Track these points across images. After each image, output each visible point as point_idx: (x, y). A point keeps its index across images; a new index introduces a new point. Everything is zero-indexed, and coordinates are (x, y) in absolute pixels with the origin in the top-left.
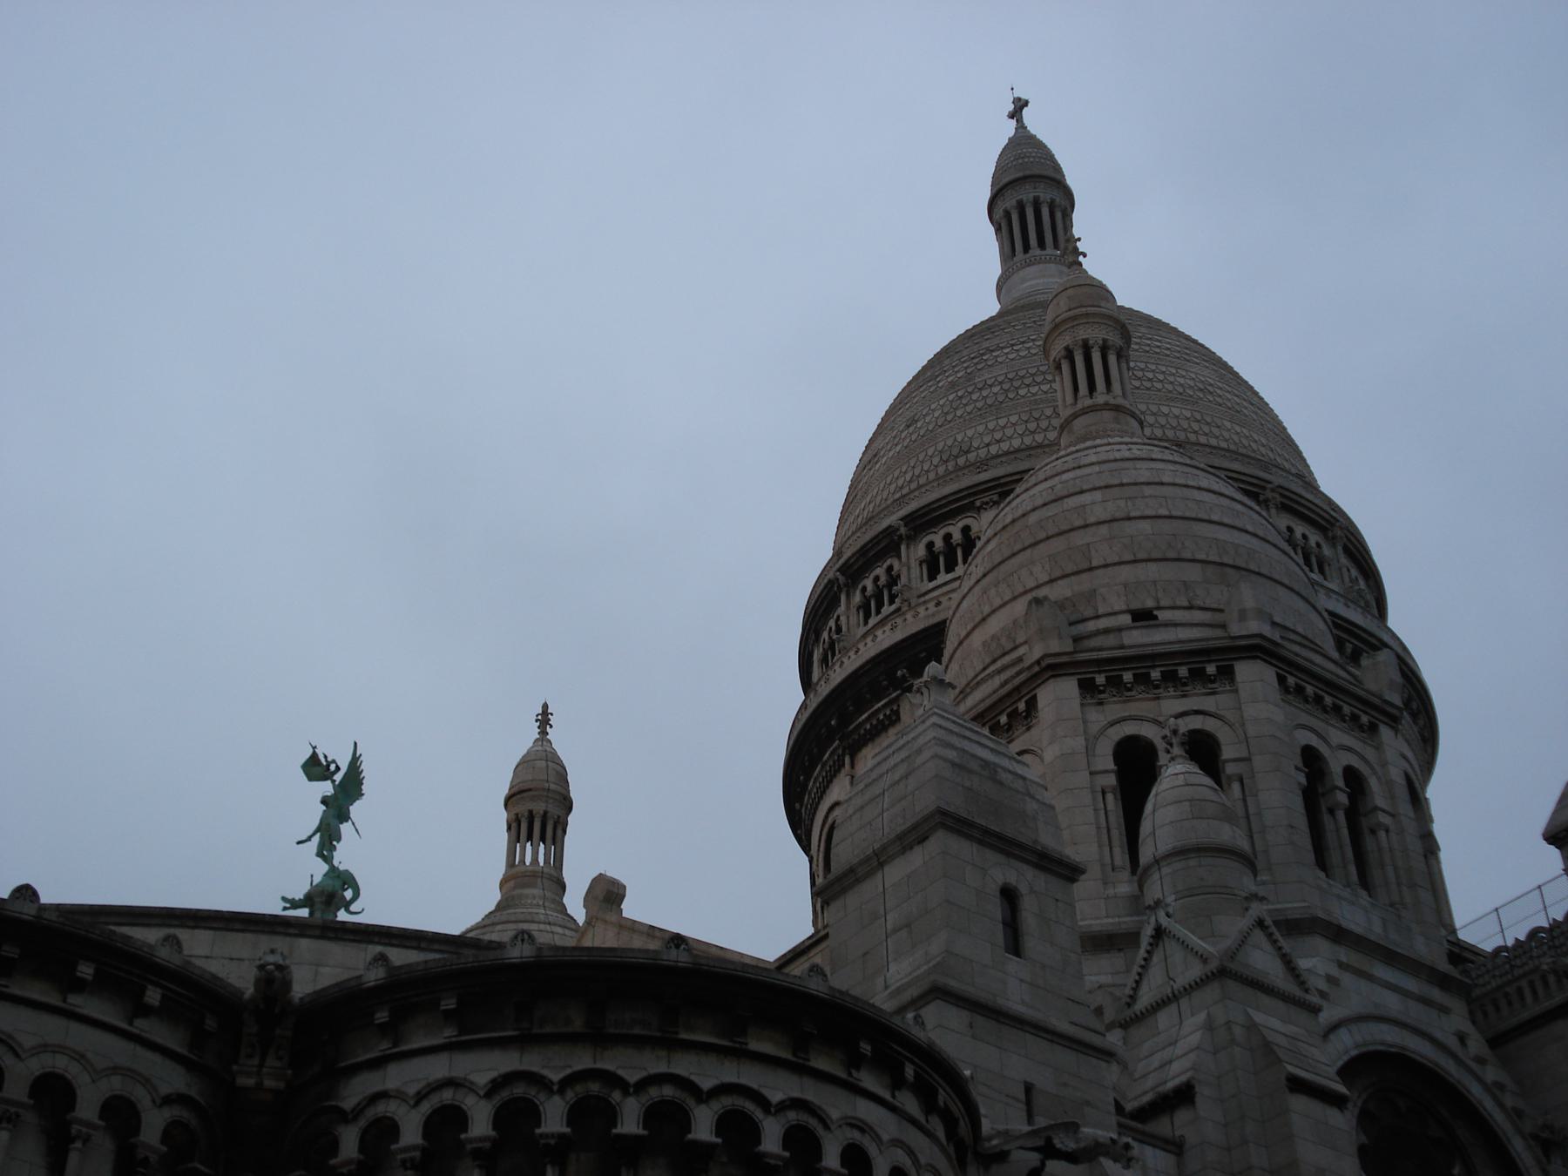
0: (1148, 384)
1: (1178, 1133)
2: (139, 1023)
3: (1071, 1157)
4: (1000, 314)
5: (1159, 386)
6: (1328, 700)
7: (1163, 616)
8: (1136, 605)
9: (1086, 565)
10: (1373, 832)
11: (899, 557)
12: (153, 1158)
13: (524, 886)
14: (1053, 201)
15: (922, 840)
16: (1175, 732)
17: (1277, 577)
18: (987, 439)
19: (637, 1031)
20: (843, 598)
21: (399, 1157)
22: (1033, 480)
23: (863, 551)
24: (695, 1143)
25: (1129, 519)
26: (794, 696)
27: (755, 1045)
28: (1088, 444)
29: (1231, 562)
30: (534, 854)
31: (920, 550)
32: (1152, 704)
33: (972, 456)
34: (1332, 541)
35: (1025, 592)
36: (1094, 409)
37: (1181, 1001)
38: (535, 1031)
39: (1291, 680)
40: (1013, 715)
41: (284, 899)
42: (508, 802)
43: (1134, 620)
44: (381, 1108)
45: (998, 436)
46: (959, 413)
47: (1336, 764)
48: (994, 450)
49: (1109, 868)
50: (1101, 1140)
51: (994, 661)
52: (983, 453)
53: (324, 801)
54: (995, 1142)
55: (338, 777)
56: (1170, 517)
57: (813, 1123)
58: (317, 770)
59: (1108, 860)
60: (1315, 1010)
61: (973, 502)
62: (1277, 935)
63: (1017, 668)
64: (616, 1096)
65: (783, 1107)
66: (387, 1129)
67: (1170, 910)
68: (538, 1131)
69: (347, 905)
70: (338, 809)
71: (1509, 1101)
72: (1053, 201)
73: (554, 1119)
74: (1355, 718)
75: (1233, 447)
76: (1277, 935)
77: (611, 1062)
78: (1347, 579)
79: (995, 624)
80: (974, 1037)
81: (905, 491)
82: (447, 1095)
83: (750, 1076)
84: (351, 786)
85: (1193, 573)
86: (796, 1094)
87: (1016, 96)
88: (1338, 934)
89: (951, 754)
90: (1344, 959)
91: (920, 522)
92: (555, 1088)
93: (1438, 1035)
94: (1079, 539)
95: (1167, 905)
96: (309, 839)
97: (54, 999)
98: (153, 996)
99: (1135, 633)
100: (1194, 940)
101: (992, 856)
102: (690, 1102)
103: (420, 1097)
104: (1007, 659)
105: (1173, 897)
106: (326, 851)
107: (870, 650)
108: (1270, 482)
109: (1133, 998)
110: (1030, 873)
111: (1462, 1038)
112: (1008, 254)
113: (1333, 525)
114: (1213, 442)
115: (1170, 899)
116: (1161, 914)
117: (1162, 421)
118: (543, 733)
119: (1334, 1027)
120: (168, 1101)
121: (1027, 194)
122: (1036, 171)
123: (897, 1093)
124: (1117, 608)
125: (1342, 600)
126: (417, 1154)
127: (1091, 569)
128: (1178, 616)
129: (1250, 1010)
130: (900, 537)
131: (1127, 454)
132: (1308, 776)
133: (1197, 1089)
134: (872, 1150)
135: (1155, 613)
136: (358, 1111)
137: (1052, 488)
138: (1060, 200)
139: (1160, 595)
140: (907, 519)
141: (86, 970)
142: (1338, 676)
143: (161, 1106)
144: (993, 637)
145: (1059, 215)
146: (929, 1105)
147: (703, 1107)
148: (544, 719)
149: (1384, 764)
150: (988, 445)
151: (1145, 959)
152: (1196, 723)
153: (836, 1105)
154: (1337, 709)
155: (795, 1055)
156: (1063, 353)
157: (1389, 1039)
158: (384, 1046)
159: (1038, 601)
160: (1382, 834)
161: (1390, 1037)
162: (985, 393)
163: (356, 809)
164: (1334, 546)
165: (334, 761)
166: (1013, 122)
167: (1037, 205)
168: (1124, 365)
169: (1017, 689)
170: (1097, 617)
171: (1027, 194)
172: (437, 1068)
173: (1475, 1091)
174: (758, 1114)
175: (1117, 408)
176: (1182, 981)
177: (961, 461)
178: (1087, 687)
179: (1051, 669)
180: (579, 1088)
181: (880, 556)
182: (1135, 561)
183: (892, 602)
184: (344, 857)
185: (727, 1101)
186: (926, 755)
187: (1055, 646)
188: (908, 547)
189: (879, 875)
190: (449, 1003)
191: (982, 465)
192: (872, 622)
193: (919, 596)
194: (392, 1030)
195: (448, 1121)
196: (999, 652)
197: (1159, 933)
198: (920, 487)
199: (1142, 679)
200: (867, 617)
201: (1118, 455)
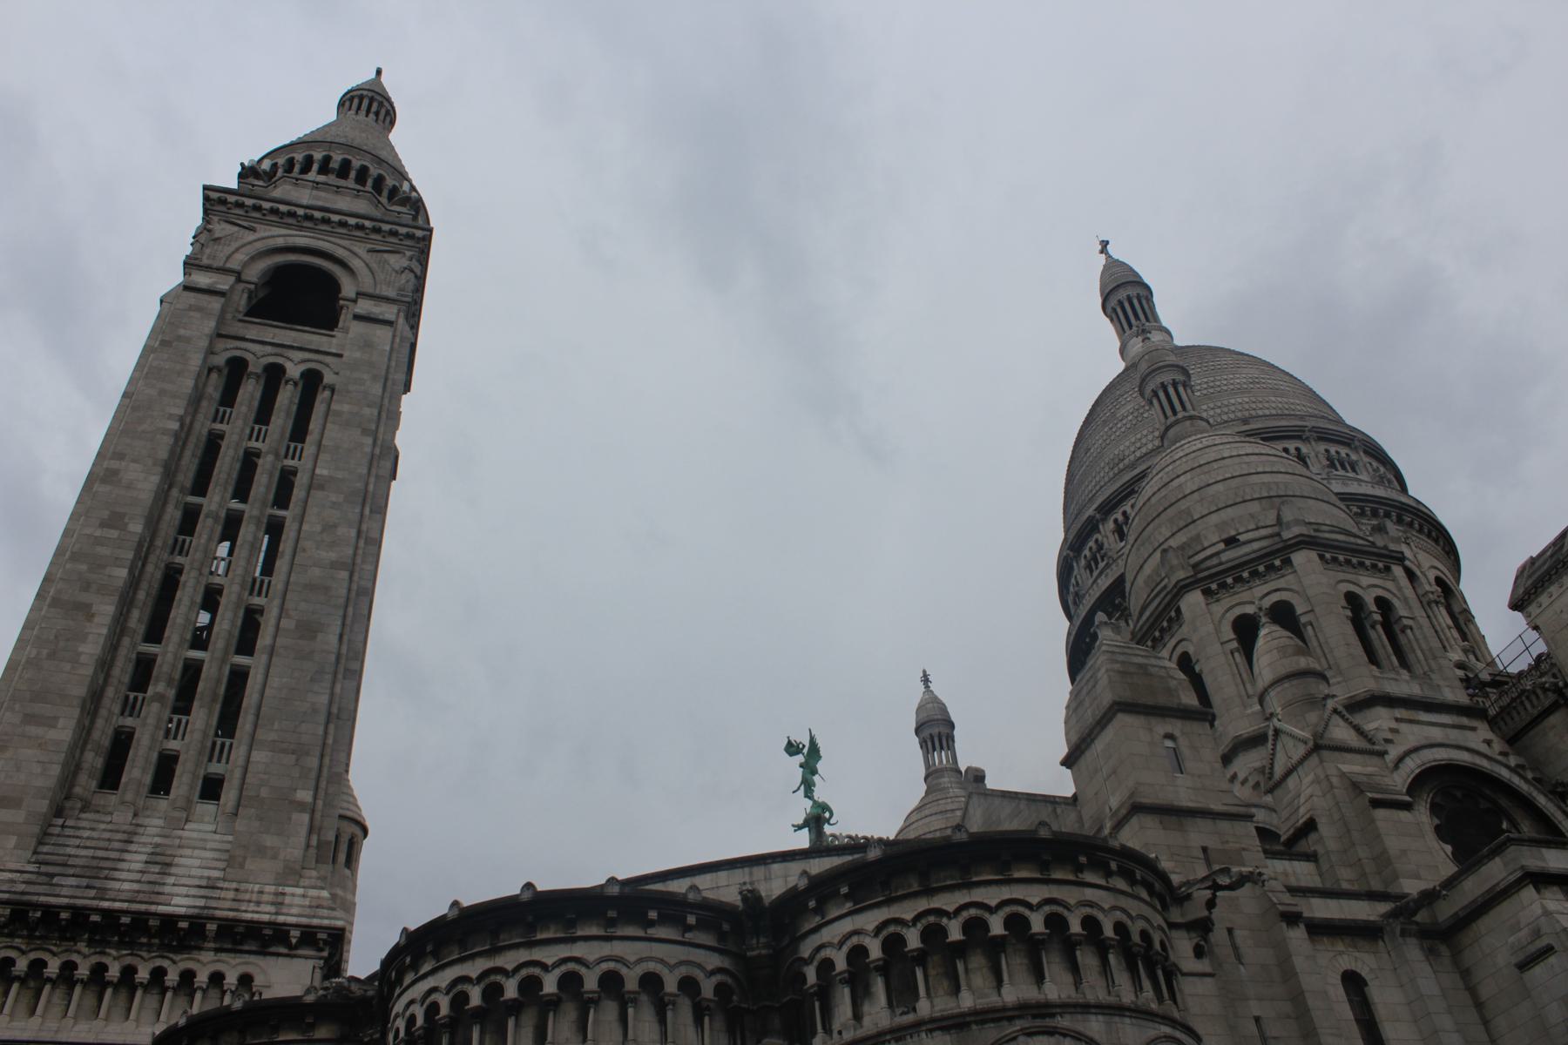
0: (1219, 389)
1: (1312, 849)
2: (687, 935)
3: (1230, 887)
4: (1126, 370)
5: (1225, 388)
6: (1354, 560)
7: (1242, 538)
8: (1225, 536)
9: (1190, 520)
10: (1403, 631)
11: (1099, 532)
12: (712, 1005)
13: (938, 778)
14: (1138, 294)
15: (1110, 720)
16: (1260, 609)
17: (1306, 494)
18: (1132, 449)
19: (949, 883)
20: (1075, 564)
21: (838, 978)
22: (1154, 472)
24: (995, 937)
25: (1209, 485)
26: (1065, 624)
27: (1017, 875)
28: (1178, 445)
29: (1275, 494)
30: (939, 759)
31: (1111, 525)
32: (1249, 592)
33: (1126, 461)
34: (1356, 449)
35: (1155, 550)
36: (1177, 422)
37: (1299, 769)
38: (893, 895)
39: (1328, 556)
40: (1170, 620)
41: (793, 826)
42: (918, 731)
43: (1226, 545)
45: (1138, 445)
46: (1112, 438)
47: (1369, 598)
48: (1138, 454)
49: (1246, 697)
50: (1244, 874)
51: (1153, 590)
52: (1132, 458)
53: (801, 766)
54: (1183, 889)
55: (805, 751)
56: (1233, 477)
57: (1060, 909)
58: (793, 749)
59: (1243, 693)
60: (1382, 754)
61: (1133, 489)
62: (1347, 716)
63: (1162, 595)
65: (1040, 905)
66: (827, 964)
67: (1280, 717)
68: (906, 950)
69: (828, 821)
70: (810, 769)
71: (1530, 775)
72: (1138, 294)
73: (913, 940)
74: (1374, 566)
75: (1279, 412)
76: (1347, 716)
77: (939, 902)
78: (1370, 470)
79: (1148, 570)
80: (1164, 828)
81: (1094, 492)
82: (855, 940)
83: (1017, 892)
84: (814, 752)
85: (1254, 507)
86: (1047, 896)
87: (1101, 239)
88: (1390, 701)
89: (1117, 666)
90: (1399, 716)
91: (1107, 508)
92: (910, 924)
93: (1473, 745)
94: (1183, 505)
95: (1277, 714)
96: (799, 788)
97: (640, 933)
98: (691, 920)
99: (1227, 553)
100: (1297, 731)
101: (1154, 721)
102: (986, 915)
103: (841, 944)
104: (1159, 588)
105: (1280, 709)
106: (809, 794)
107: (1096, 593)
108: (1306, 427)
109: (1271, 774)
111: (1488, 742)
112: (1121, 332)
113: (1353, 440)
114: (1267, 412)
115: (1279, 710)
116: (1275, 720)
117: (1233, 408)
118: (927, 687)
119: (1401, 759)
120: (713, 973)
121: (1122, 294)
122: (1124, 281)
123: (1109, 879)
124: (1215, 541)
125: (1370, 485)
126: (846, 975)
127: (1194, 521)
128: (1251, 535)
129: (1339, 765)
130: (1097, 521)
131: (1200, 446)
132: (1352, 611)
133: (1317, 820)
134: (1100, 916)
135: (1238, 537)
136: (812, 957)
137: (1161, 478)
138: (1143, 293)
139: (1238, 526)
140: (1098, 509)
141: (653, 915)
142: (1358, 545)
143: (710, 976)
144: (1149, 577)
145: (1144, 302)
146: (1132, 881)
147: (994, 916)
148: (926, 679)
149: (1400, 589)
150: (1134, 452)
151: (1273, 749)
152: (1275, 597)
153: (1070, 895)
154: (1361, 564)
155: (1042, 874)
156: (1152, 394)
157: (1438, 756)
158: (817, 920)
159: (1165, 551)
160: (1409, 631)
161: (1441, 755)
162: (1124, 422)
163: (820, 766)
164: (1357, 452)
165: (800, 743)
166: (1104, 255)
167: (1129, 299)
168: (1189, 391)
169: (1169, 604)
170: (1204, 549)
171: (1122, 294)
172: (846, 925)
173: (1505, 773)
174: (1027, 912)
175: (1191, 418)
176: (1296, 757)
177: (1121, 466)
178: (1207, 593)
179: (1182, 589)
180: (924, 921)
181: (1089, 535)
182: (1219, 510)
183: (1103, 560)
184: (820, 794)
185: (1008, 910)
186: (1103, 670)
187: (1181, 574)
188: (1103, 524)
189: (1093, 746)
190: (844, 890)
191: (1133, 466)
192: (1095, 573)
193: (1117, 553)
194: (819, 910)
196: (1154, 584)
197: (1277, 732)
198: (1101, 487)
199: (1239, 580)
200: (1091, 572)
201: (1194, 448)
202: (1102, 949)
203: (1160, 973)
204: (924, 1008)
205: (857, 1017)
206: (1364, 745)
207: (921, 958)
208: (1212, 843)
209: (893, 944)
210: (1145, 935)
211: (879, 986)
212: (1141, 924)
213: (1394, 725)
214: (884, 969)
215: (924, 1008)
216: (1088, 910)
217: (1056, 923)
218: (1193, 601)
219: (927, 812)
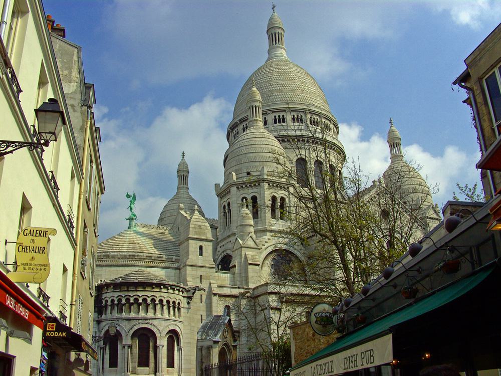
23: (233, 125)
31: (242, 127)
44: (106, 299)
55: (132, 197)
64: (130, 298)
66: (107, 301)
73: (124, 301)
82: (112, 298)
94: (241, 157)
101: (198, 241)
110: (204, 242)
118: (183, 158)
134: (163, 299)
140: (239, 120)
145: (280, 35)
146: (174, 290)
148: (183, 155)
152: (254, 194)
153: (158, 295)
172: (111, 294)
175: (257, 120)
178: (238, 188)
181: (236, 127)
190: (112, 287)
192: (235, 140)
195: (113, 301)
199: (246, 186)
202: (162, 306)
203: (176, 309)
204: (124, 315)
205: (111, 313)
206: (256, 246)
207: (124, 304)
208: (203, 274)
209: (120, 300)
210: (174, 302)
211: (116, 308)
212: (174, 300)
213: (270, 237)
214: (117, 305)
215: (124, 315)
216: (161, 298)
217: (153, 301)
218: (234, 189)
219: (174, 202)
